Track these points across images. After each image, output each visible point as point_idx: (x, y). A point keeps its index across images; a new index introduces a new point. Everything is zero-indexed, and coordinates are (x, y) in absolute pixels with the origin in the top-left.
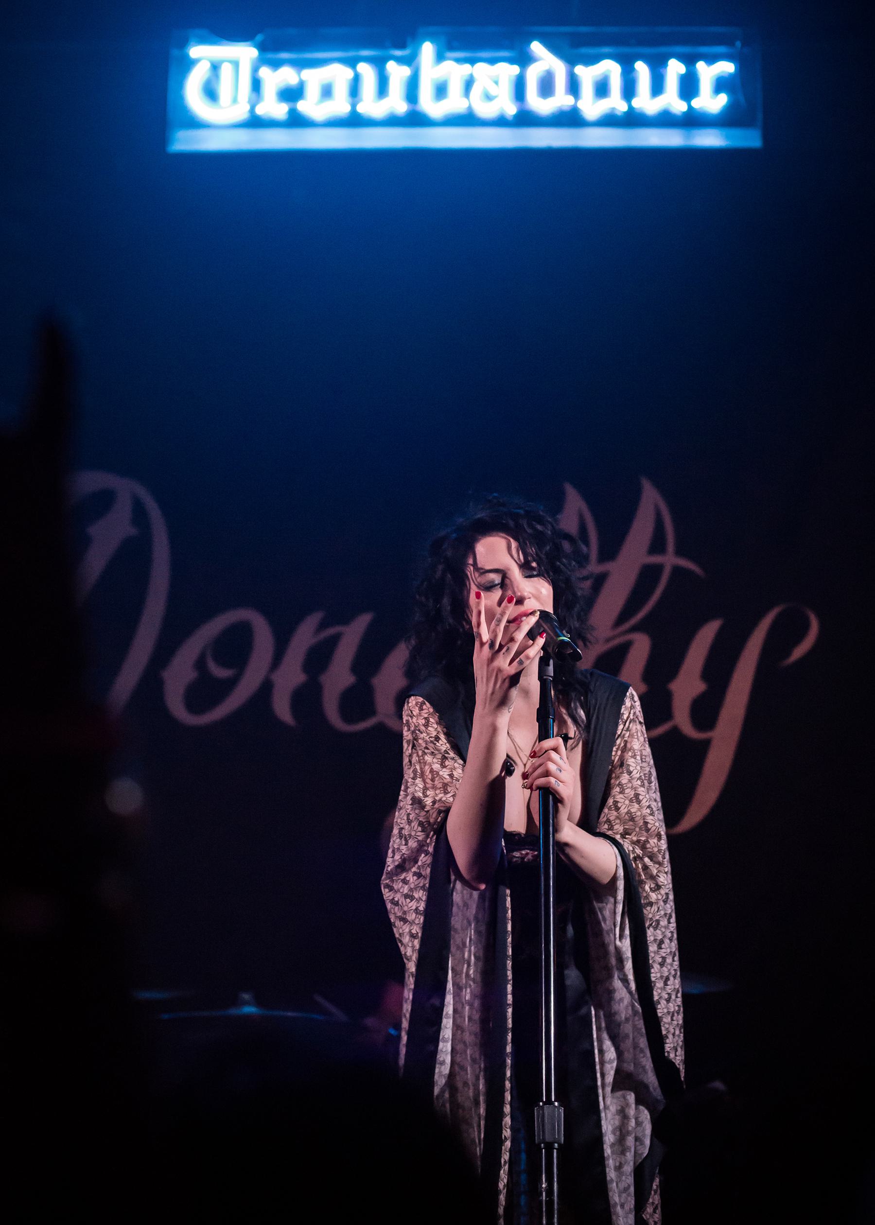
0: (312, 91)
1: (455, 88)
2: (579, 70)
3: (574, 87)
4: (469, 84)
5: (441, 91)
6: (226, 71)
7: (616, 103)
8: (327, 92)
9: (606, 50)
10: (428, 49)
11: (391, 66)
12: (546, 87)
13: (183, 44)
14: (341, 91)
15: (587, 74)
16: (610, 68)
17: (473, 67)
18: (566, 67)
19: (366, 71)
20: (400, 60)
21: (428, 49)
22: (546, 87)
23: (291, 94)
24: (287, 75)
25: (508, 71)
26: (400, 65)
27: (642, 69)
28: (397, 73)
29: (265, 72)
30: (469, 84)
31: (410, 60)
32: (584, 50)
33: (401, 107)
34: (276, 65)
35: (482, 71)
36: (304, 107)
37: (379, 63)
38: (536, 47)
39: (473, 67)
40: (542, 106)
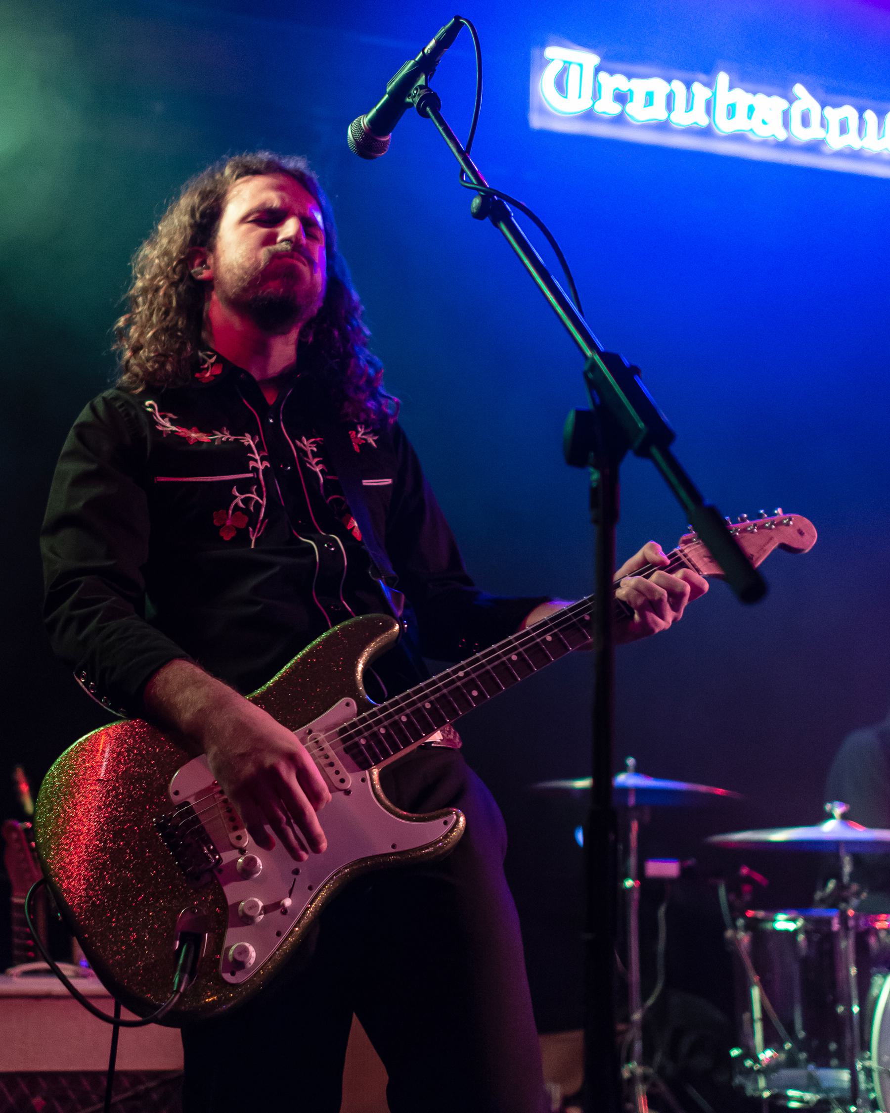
1: (741, 112)
2: (828, 109)
3: (823, 124)
4: (751, 109)
5: (731, 112)
6: (573, 72)
7: (852, 141)
8: (649, 100)
10: (723, 78)
11: (697, 87)
12: (805, 121)
13: (543, 45)
15: (834, 115)
16: (848, 112)
19: (678, 86)
21: (723, 78)
22: (805, 121)
23: (621, 98)
24: (619, 82)
25: (778, 103)
27: (870, 116)
28: (700, 91)
29: (603, 76)
30: (751, 109)
31: (710, 84)
33: (703, 121)
34: (612, 73)
35: (760, 100)
37: (688, 85)
38: (799, 89)
40: (802, 135)
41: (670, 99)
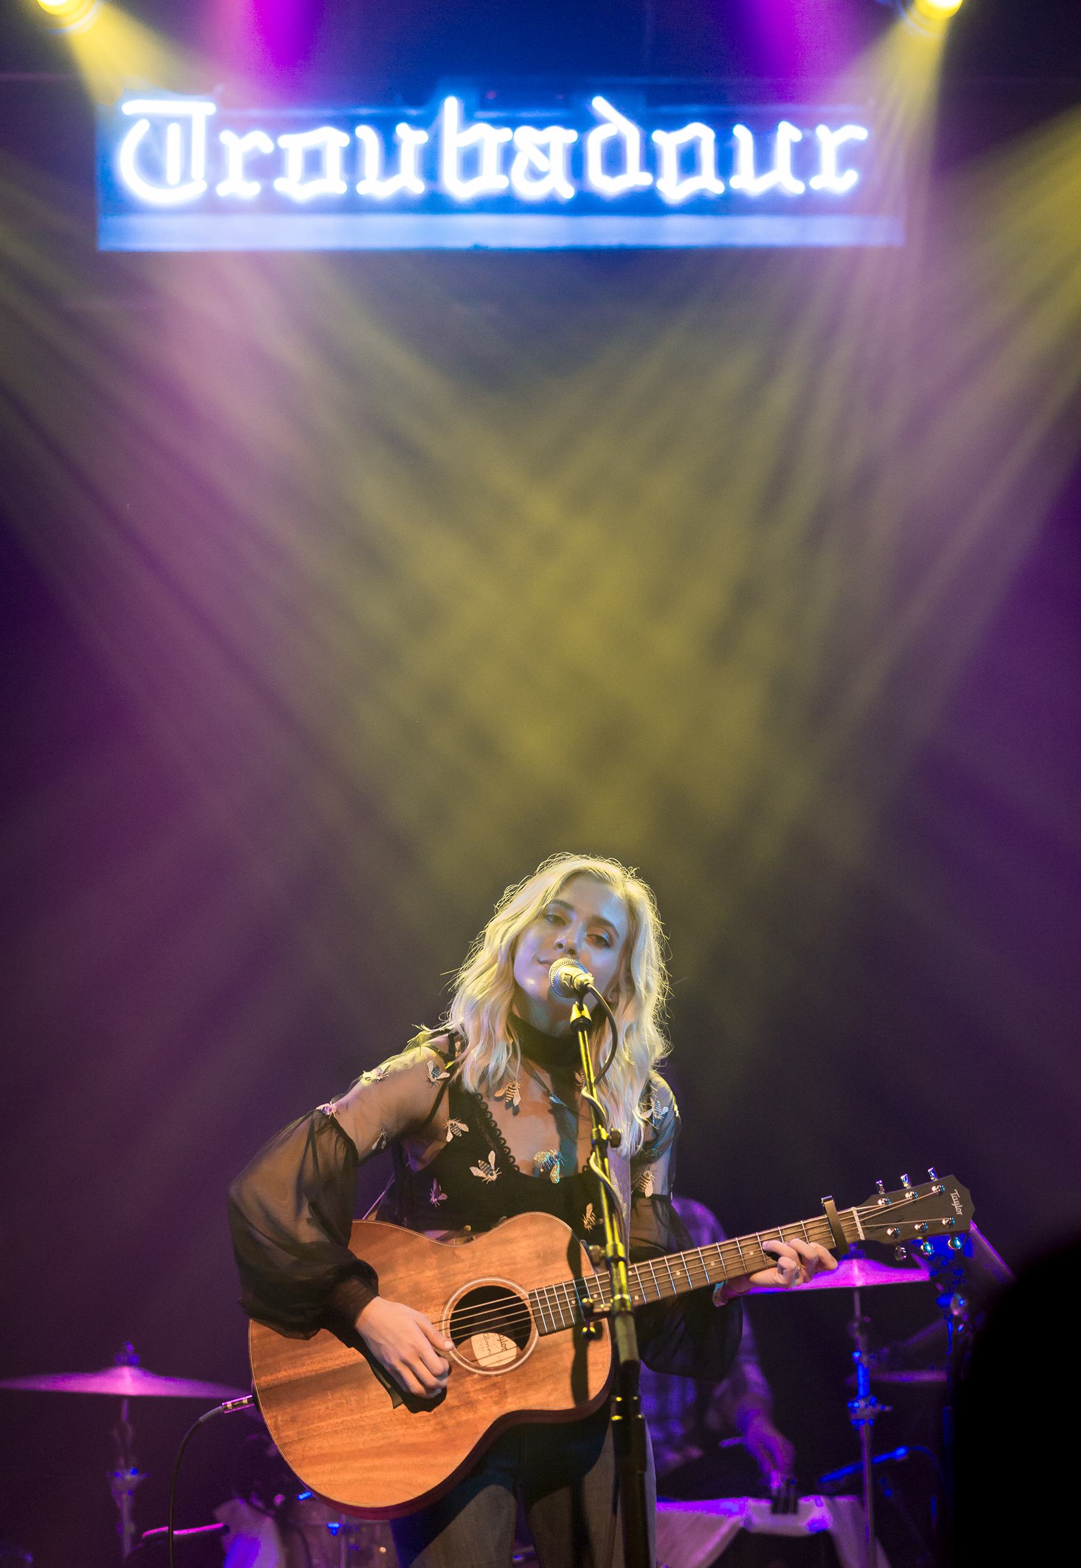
0: (295, 164)
9: (694, 109)
10: (451, 107)
11: (403, 130)
14: (333, 162)
17: (513, 132)
18: (640, 132)
19: (366, 134)
20: (417, 123)
21: (451, 107)
26: (413, 129)
31: (427, 121)
32: (666, 110)
36: (280, 185)
37: (386, 128)
38: (600, 105)
39: (513, 132)
41: (352, 156)
